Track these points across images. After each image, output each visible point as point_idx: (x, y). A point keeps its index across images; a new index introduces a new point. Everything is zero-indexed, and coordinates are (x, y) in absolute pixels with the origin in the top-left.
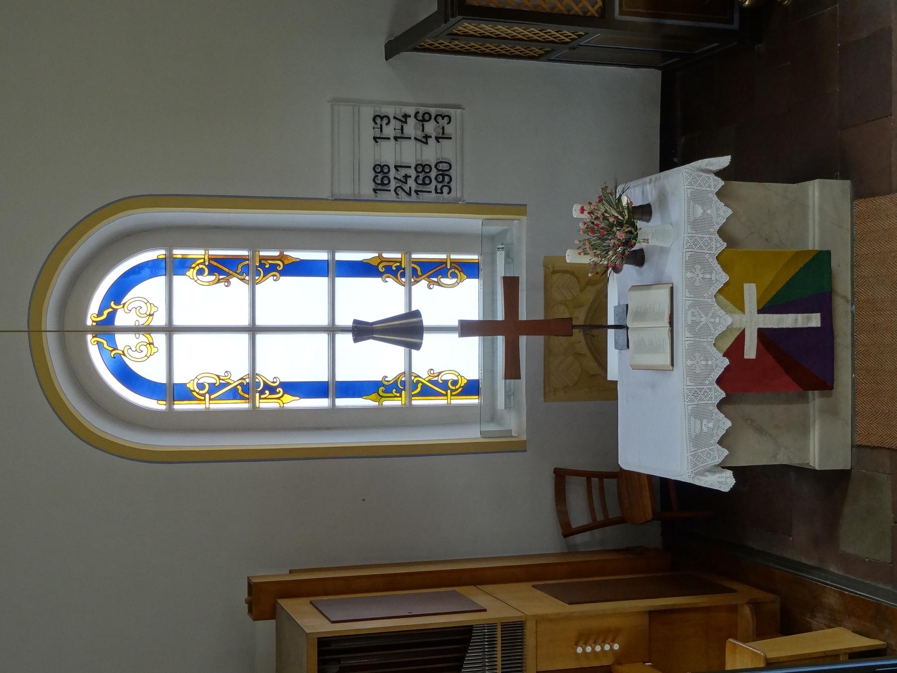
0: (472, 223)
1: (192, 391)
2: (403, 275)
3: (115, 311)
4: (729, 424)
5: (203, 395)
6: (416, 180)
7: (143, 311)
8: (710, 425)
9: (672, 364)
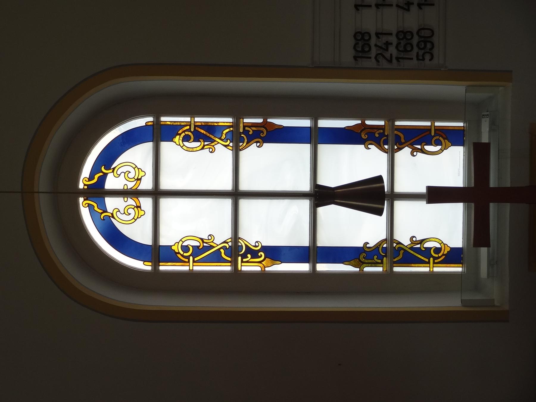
0: (454, 89)
1: (176, 253)
3: (105, 175)
5: (188, 257)
6: (397, 47)
7: (131, 175)
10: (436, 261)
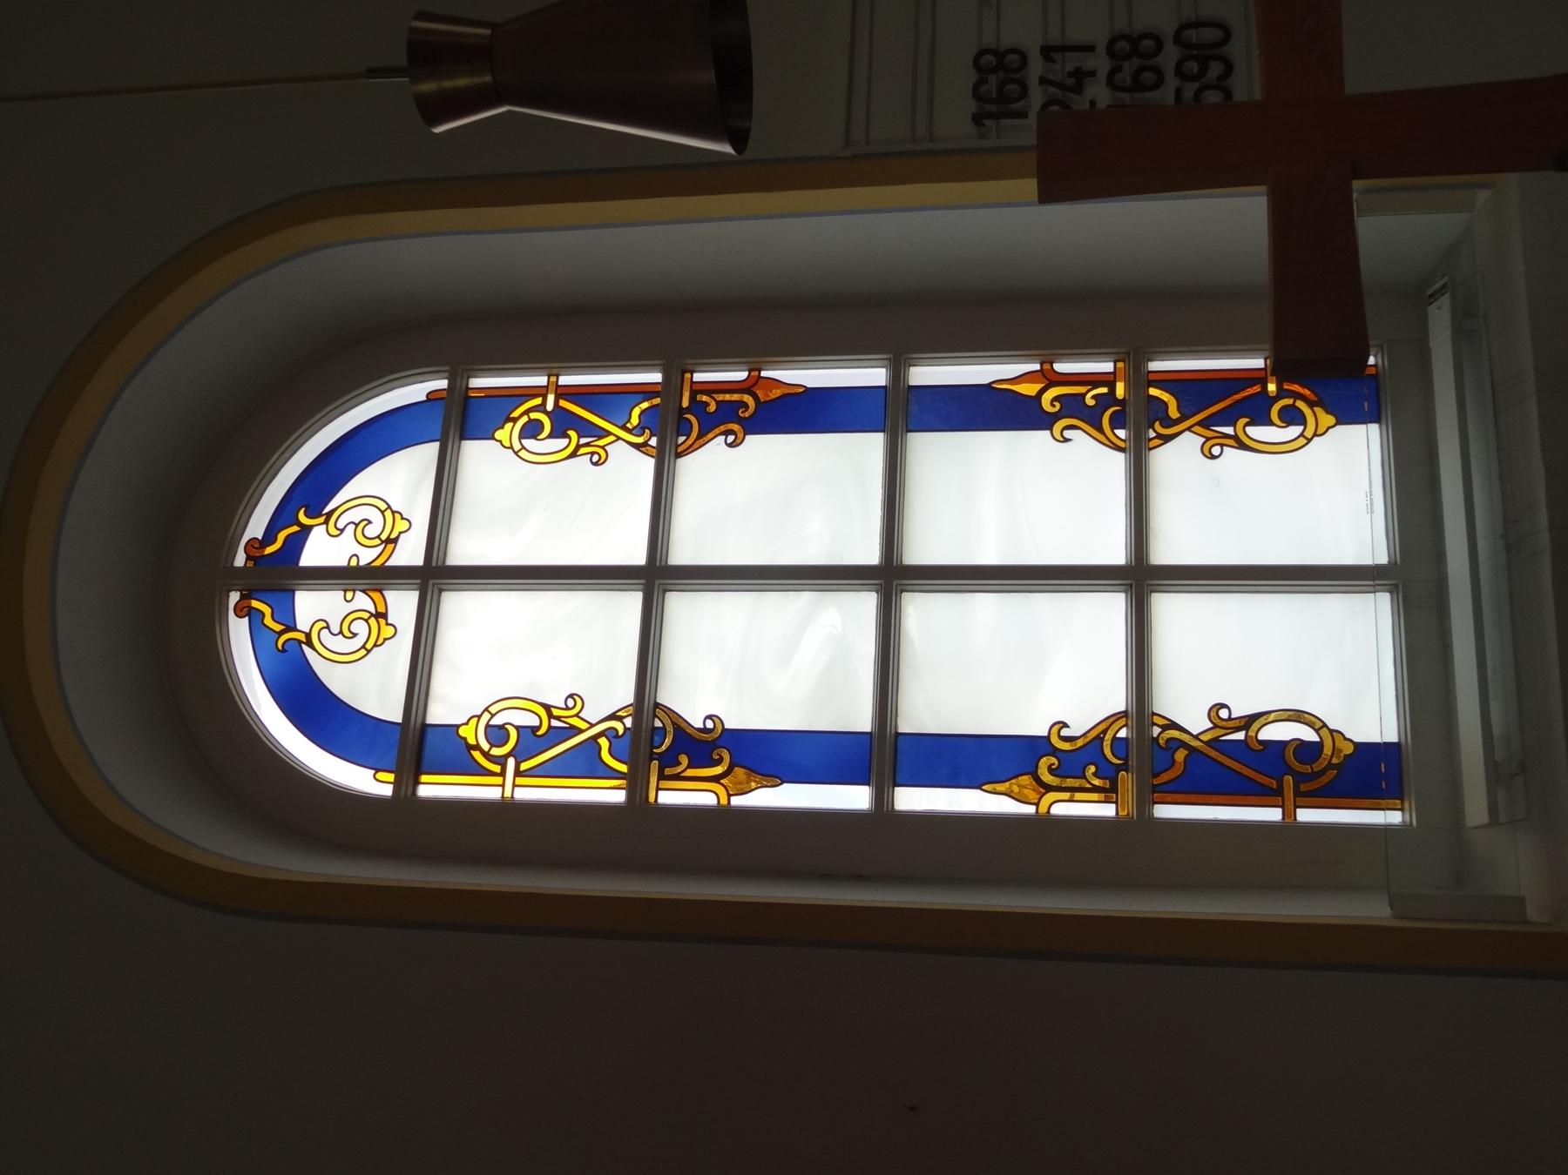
1: (470, 748)
2: (1116, 422)
3: (306, 530)
5: (501, 761)
6: (1110, 82)
7: (372, 531)
10: (1303, 788)
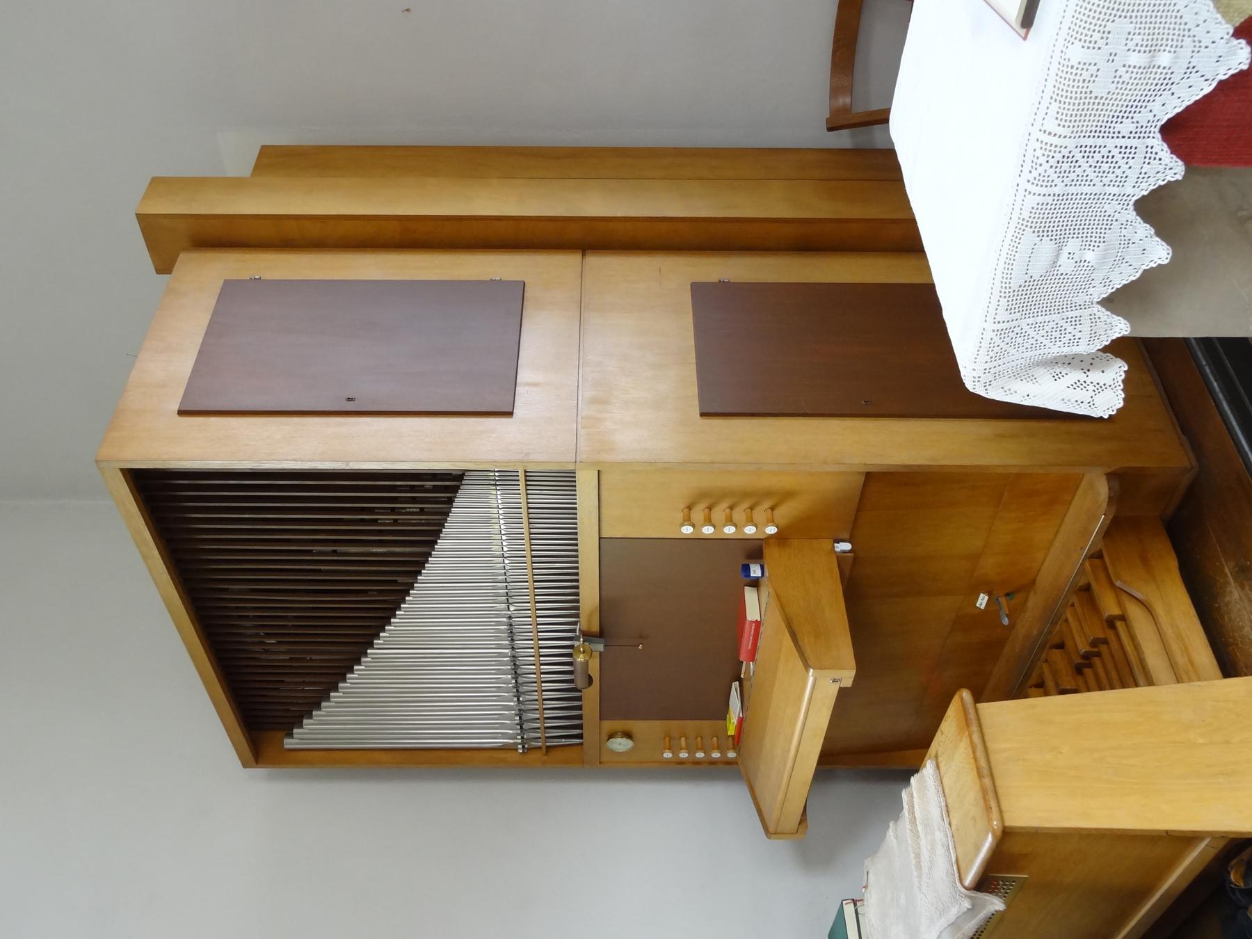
4: (1160, 253)
8: (1090, 256)
9: (1028, 19)
